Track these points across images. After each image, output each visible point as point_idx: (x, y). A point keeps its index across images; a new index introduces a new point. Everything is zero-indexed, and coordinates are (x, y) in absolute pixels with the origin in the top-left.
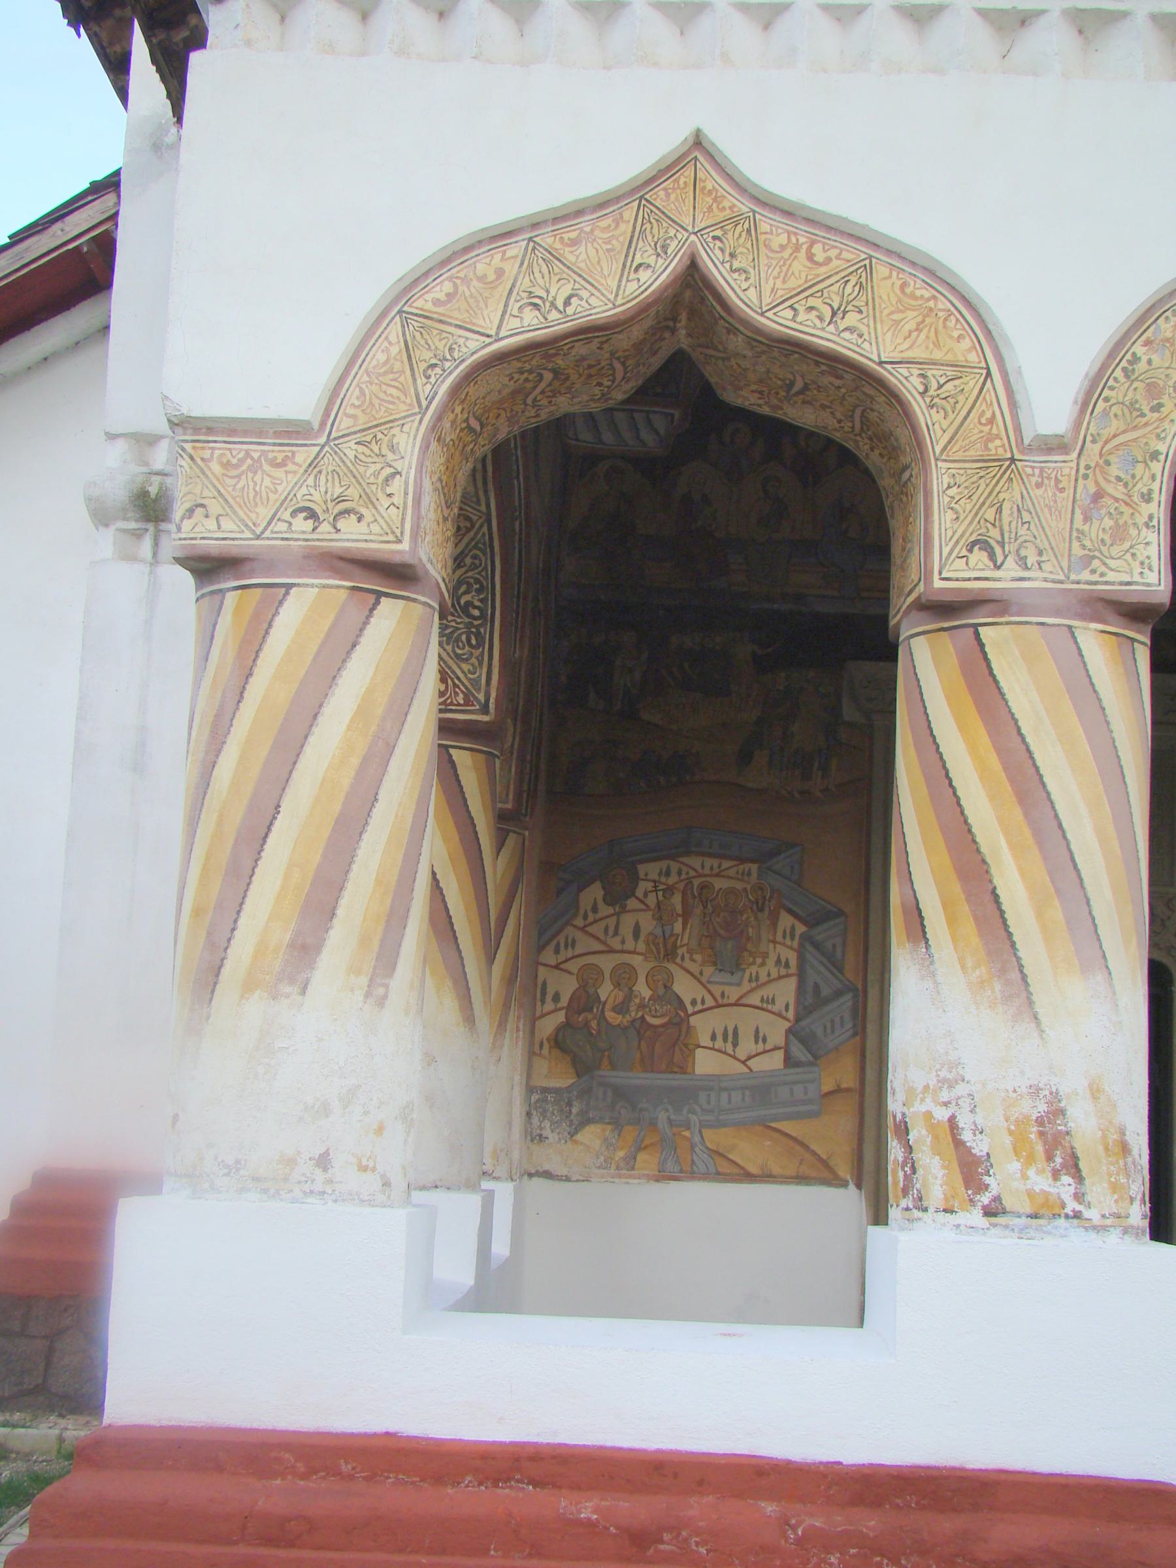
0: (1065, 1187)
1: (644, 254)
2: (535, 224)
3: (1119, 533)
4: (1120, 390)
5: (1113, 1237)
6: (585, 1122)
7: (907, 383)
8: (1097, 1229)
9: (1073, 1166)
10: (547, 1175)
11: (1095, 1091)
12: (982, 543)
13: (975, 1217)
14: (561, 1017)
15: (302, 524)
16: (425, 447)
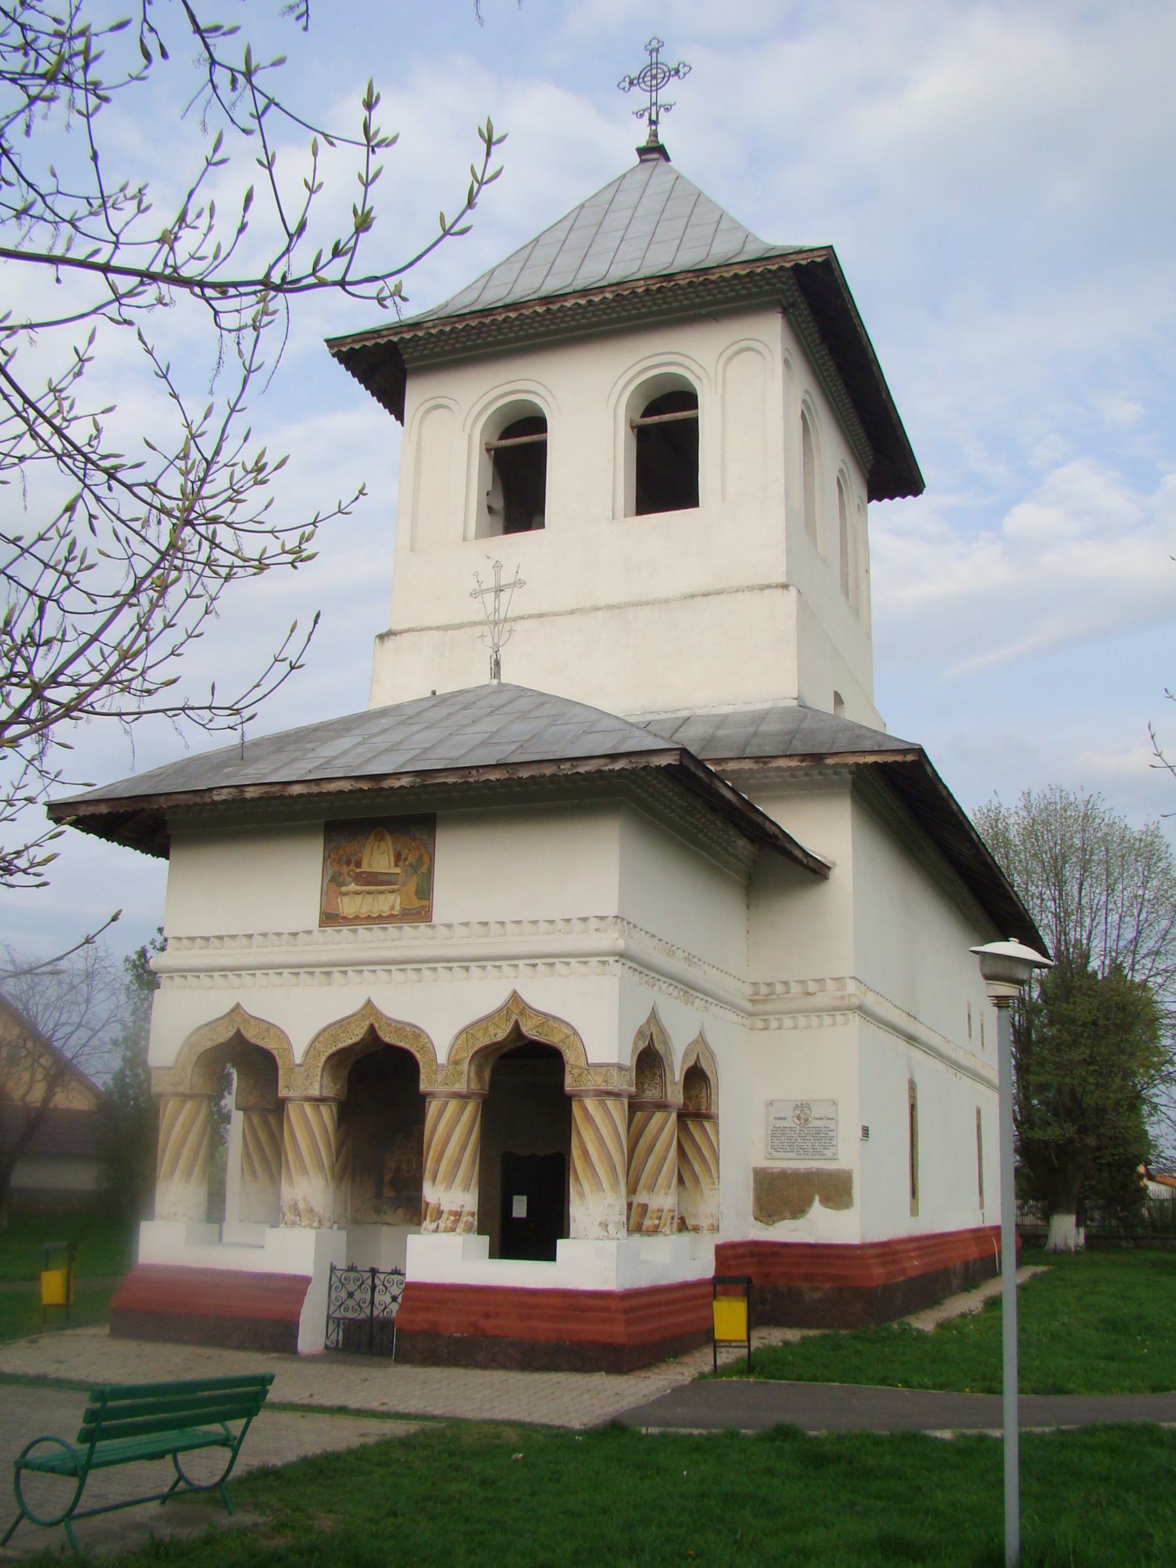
0: (298, 1218)
1: (230, 1028)
2: (211, 1022)
3: (311, 1083)
4: (313, 1053)
5: (308, 1229)
6: (398, 1207)
7: (275, 1053)
8: (305, 1227)
9: (299, 1215)
10: (387, 1224)
11: (304, 1199)
12: (287, 1087)
13: (283, 1225)
14: (392, 1175)
15: (172, 1087)
16: (193, 1071)
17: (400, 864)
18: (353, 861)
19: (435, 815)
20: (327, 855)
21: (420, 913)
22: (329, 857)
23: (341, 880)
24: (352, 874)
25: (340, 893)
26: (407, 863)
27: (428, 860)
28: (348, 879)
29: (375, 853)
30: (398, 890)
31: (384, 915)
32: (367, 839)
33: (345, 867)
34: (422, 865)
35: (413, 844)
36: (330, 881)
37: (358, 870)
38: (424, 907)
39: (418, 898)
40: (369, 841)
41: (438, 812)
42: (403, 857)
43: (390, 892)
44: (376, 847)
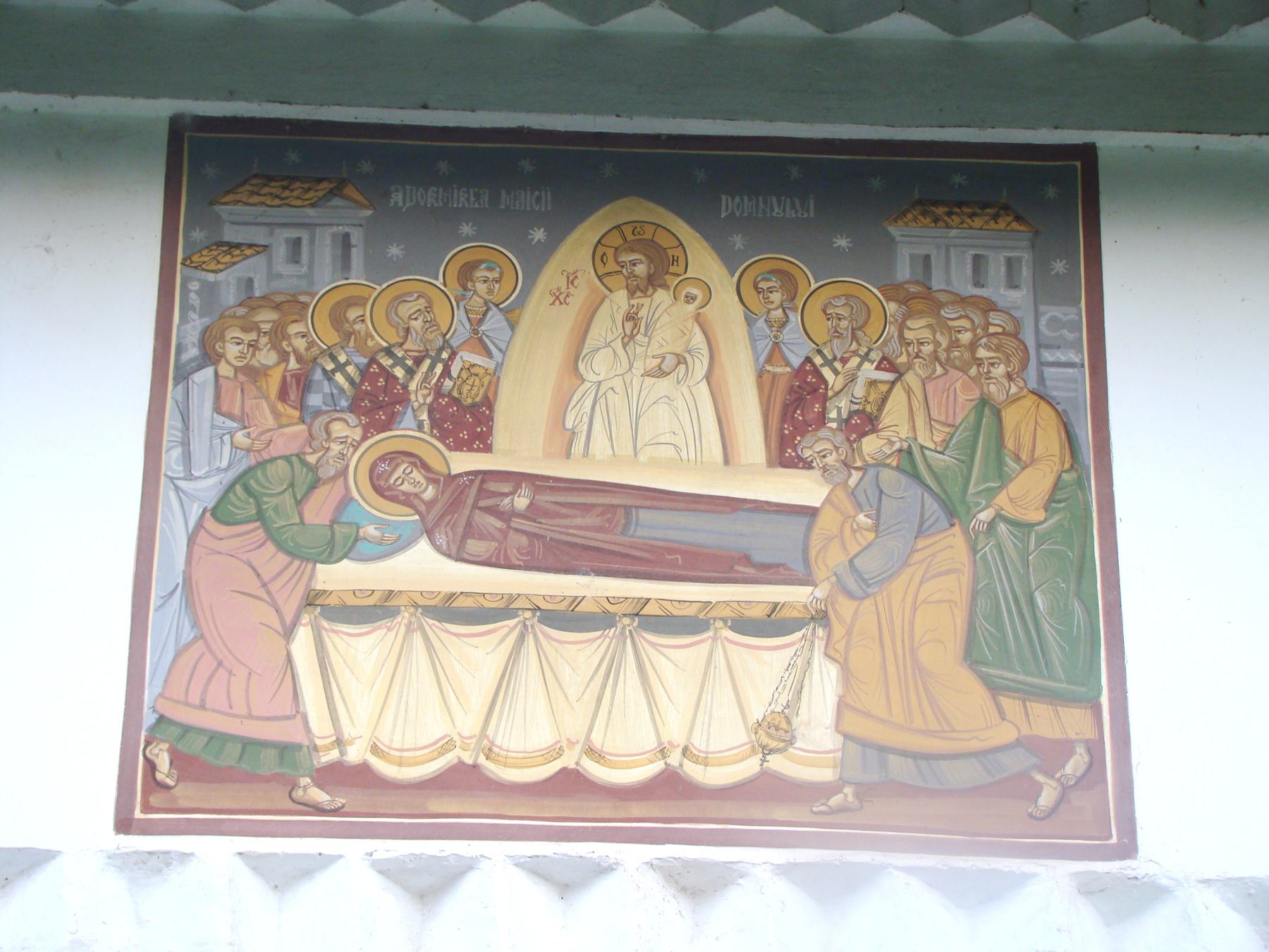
17: (810, 447)
18: (419, 394)
19: (1088, 153)
20: (188, 332)
21: (1024, 788)
22: (210, 356)
23: (318, 510)
24: (409, 480)
25: (312, 600)
26: (870, 445)
27: (1050, 442)
28: (368, 506)
29: (599, 366)
30: (821, 617)
31: (694, 772)
32: (535, 261)
33: (346, 428)
34: (1004, 479)
35: (918, 328)
36: (219, 512)
37: (463, 462)
38: (1057, 751)
39: (994, 688)
40: (551, 276)
41: (1110, 142)
42: (839, 408)
43: (745, 625)
44: (606, 326)
